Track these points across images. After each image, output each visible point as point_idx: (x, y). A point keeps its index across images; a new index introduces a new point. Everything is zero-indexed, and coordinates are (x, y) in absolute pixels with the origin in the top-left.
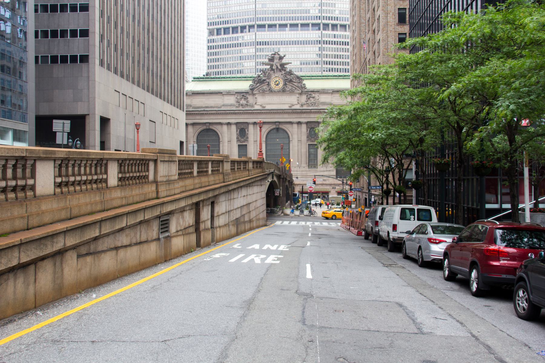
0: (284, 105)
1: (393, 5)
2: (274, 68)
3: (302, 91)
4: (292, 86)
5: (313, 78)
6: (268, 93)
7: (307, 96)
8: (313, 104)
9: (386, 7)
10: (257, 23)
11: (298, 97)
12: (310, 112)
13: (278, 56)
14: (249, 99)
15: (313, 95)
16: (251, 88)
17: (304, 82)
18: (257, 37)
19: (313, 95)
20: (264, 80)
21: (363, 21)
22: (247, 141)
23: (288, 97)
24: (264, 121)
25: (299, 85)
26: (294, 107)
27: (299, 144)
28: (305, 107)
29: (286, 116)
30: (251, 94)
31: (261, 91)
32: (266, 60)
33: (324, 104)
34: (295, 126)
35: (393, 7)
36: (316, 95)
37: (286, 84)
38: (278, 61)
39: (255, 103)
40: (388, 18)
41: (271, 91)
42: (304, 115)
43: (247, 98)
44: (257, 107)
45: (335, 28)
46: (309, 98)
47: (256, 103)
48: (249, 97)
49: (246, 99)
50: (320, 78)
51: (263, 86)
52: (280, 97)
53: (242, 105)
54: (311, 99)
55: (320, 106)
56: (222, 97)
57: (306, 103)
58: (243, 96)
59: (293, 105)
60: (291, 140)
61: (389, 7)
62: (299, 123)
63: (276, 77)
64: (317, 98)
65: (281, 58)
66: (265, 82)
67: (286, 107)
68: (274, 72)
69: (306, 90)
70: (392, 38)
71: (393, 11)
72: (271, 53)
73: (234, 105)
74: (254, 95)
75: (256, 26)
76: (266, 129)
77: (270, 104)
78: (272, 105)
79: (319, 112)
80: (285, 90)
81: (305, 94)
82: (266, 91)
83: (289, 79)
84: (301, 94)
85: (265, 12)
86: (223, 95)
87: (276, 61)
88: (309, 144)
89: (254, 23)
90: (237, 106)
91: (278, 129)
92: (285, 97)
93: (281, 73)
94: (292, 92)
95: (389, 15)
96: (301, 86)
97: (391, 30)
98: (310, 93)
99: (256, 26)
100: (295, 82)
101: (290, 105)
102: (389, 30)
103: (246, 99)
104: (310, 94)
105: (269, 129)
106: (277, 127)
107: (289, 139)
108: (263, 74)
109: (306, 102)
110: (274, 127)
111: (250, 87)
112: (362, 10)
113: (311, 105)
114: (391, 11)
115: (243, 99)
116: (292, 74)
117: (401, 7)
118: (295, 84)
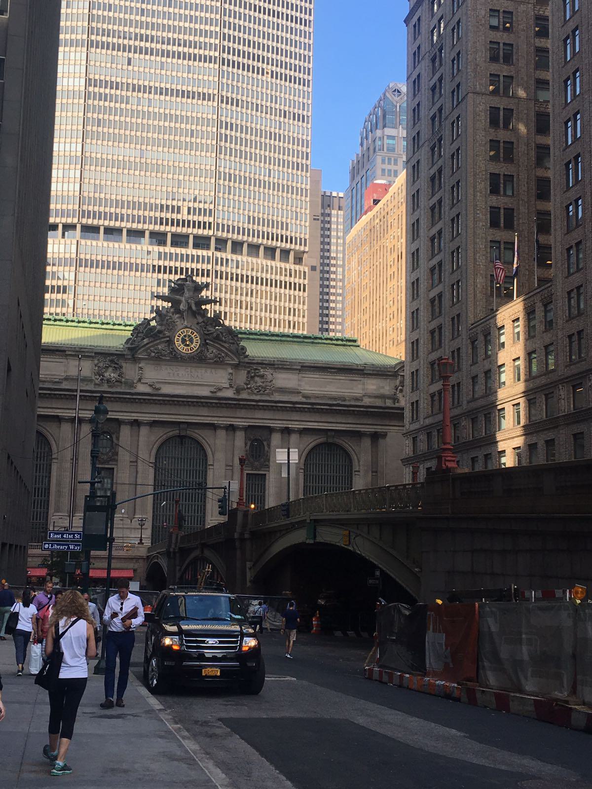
0: (200, 388)
2: (181, 307)
3: (239, 362)
4: (218, 349)
5: (251, 337)
6: (168, 361)
7: (249, 372)
8: (260, 390)
10: (84, 221)
11: (232, 374)
12: (254, 406)
13: (193, 285)
14: (124, 370)
15: (262, 372)
16: (129, 346)
17: (242, 343)
18: (81, 249)
19: (262, 372)
20: (160, 332)
22: (117, 461)
23: (209, 371)
24: (157, 419)
25: (233, 347)
26: (220, 394)
27: (230, 472)
28: (244, 395)
29: (204, 411)
30: (129, 359)
31: (153, 354)
32: (166, 291)
33: (282, 390)
34: (222, 433)
36: (268, 373)
37: (207, 344)
38: (191, 293)
39: (137, 378)
41: (176, 358)
42: (242, 413)
43: (121, 367)
44: (141, 388)
45: (238, 248)
46: (252, 377)
47: (140, 380)
48: (124, 365)
49: (118, 368)
50: (266, 338)
51: (157, 344)
52: (193, 370)
53: (108, 381)
54: (257, 379)
55: (276, 394)
56: (65, 360)
57: (245, 387)
58: (112, 361)
59: (220, 390)
60: (210, 462)
62: (232, 428)
63: (186, 327)
64: (270, 377)
65: (198, 288)
66: (161, 336)
67: (205, 392)
68: (182, 317)
69: (246, 360)
72: (177, 277)
73: (91, 381)
74: (135, 360)
75: (79, 227)
76: (160, 434)
77: (169, 383)
78: (176, 387)
79: (274, 407)
80: (206, 357)
81: (245, 367)
82: (165, 356)
83: (215, 335)
84: (236, 367)
85: (99, 202)
86: (67, 355)
87: (187, 294)
88: (247, 474)
89: (75, 221)
90: (97, 382)
91: (182, 438)
92: (203, 371)
93: (195, 321)
94: (219, 363)
96: (237, 350)
98: (254, 367)
99: (79, 227)
100: (225, 342)
101: (212, 389)
103: (118, 368)
104: (256, 369)
105: (164, 437)
106: (183, 434)
107: (206, 460)
108: (158, 318)
109: (247, 384)
110: (176, 432)
111: (127, 342)
113: (255, 391)
115: (110, 369)
116: (219, 324)
118: (226, 345)
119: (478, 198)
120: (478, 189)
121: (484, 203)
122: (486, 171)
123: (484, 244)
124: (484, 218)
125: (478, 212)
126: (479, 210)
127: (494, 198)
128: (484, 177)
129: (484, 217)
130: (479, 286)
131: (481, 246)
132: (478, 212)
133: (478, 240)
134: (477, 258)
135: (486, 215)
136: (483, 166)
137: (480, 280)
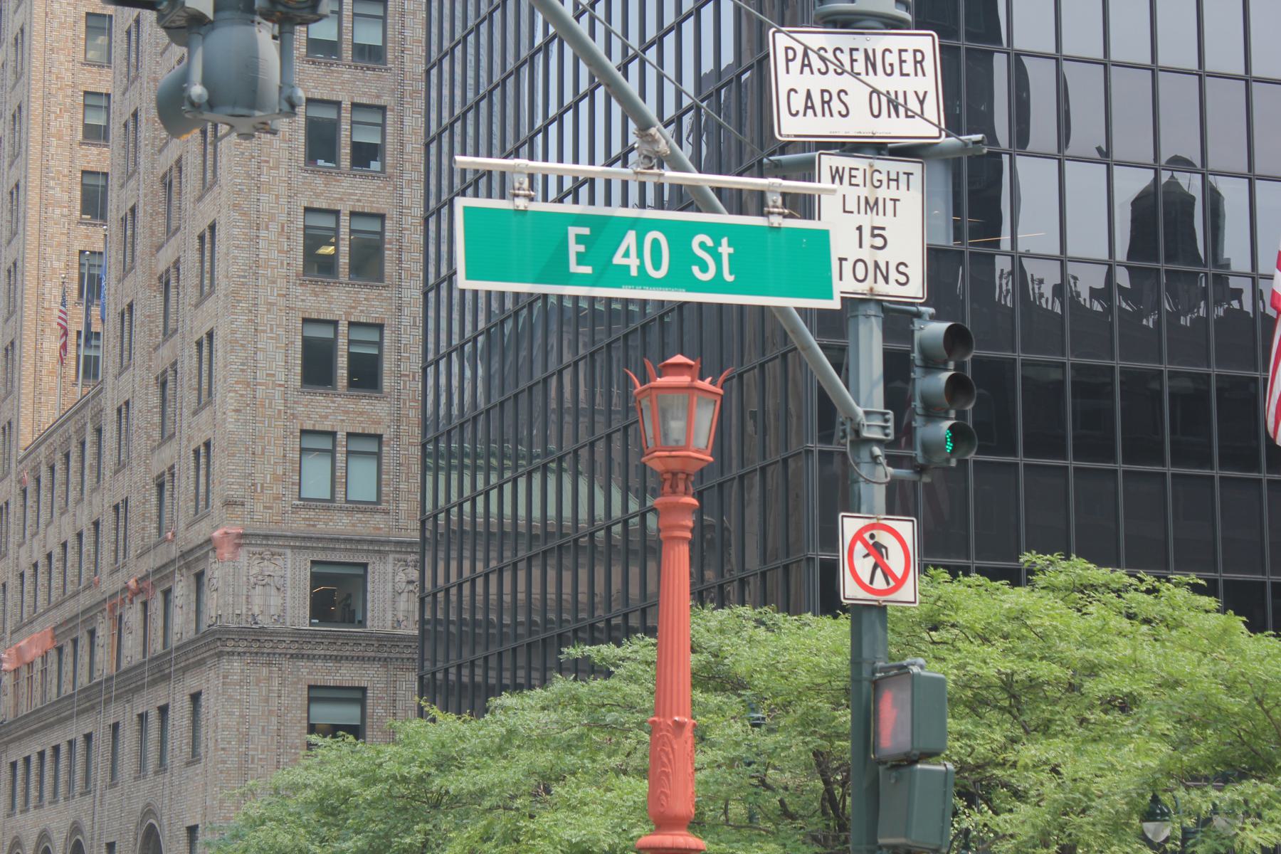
1: (283, 189)
9: (254, 196)
21: (57, 193)
35: (283, 201)
40: (262, 244)
61: (264, 198)
70: (277, 338)
71: (283, 218)
95: (263, 233)
97: (272, 299)
102: (261, 301)
112: (54, 141)
114: (272, 218)
117: (316, 205)
119: (52, 150)
120: (53, 130)
121: (67, 163)
122: (74, 86)
123: (64, 258)
124: (68, 196)
125: (52, 183)
126: (53, 179)
127: (94, 150)
128: (68, 101)
129: (66, 197)
130: (46, 358)
131: (56, 264)
132: (52, 183)
133: (49, 250)
134: (46, 291)
135: (70, 191)
136: (68, 76)
137: (52, 345)
